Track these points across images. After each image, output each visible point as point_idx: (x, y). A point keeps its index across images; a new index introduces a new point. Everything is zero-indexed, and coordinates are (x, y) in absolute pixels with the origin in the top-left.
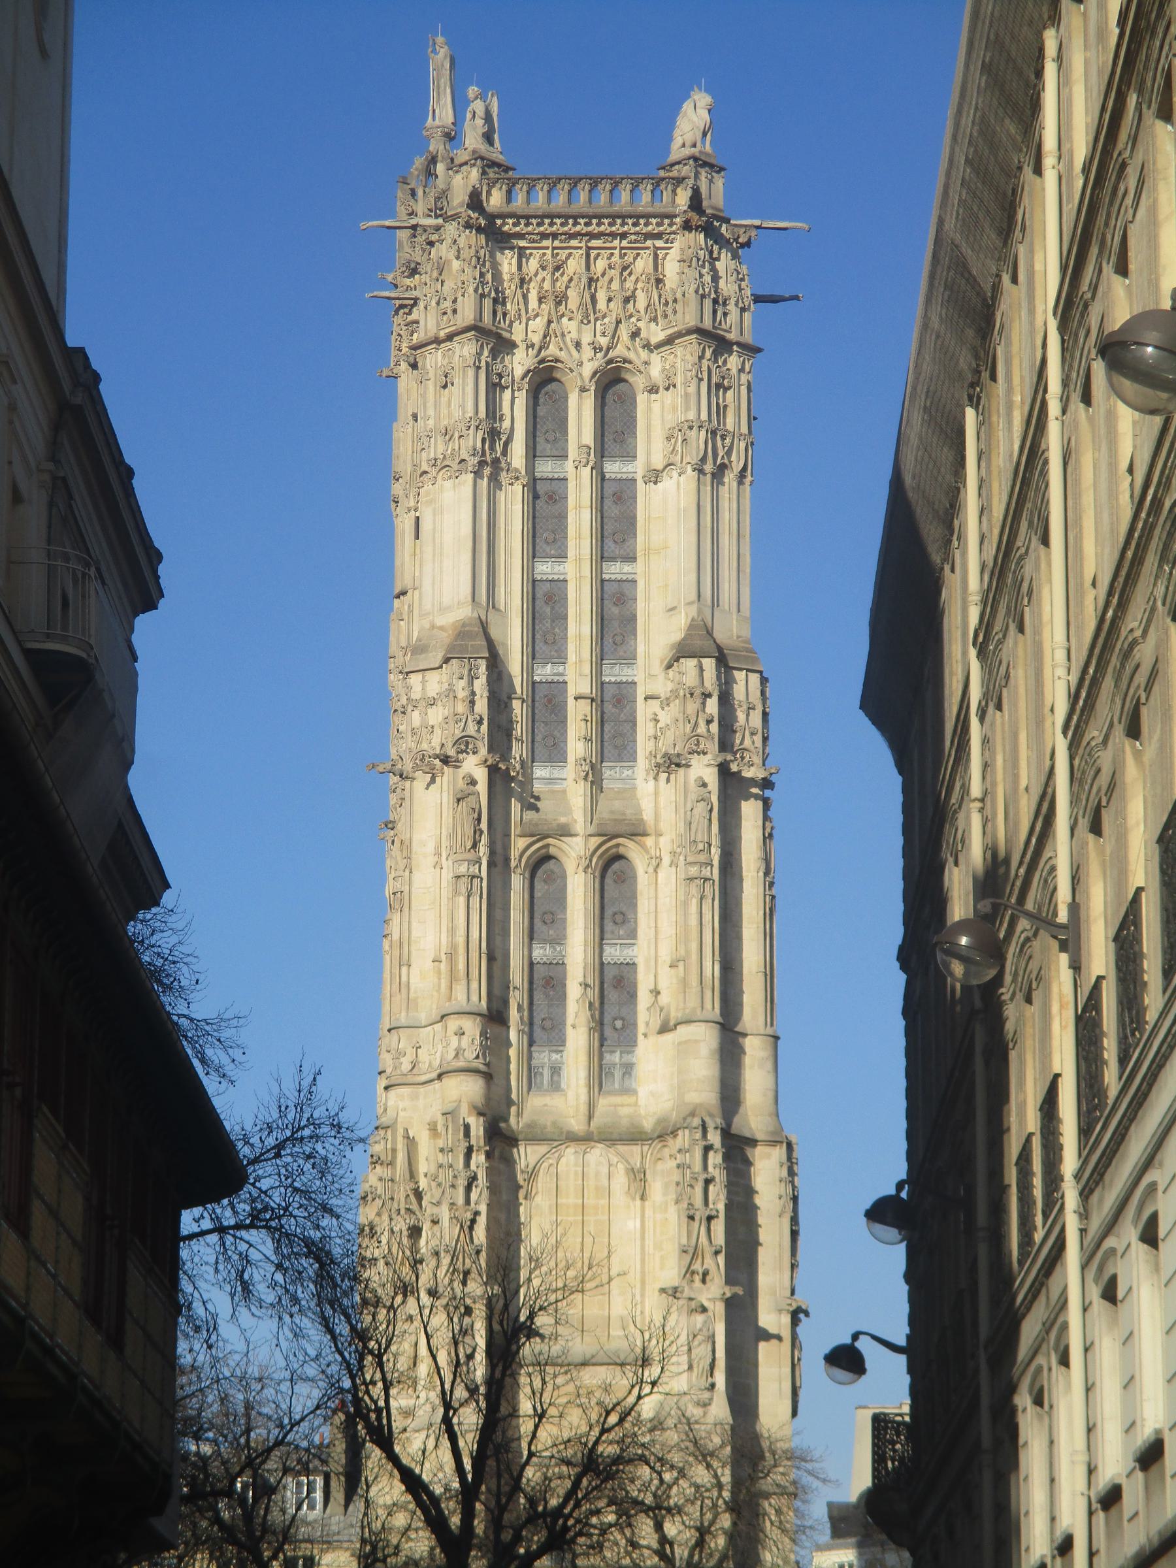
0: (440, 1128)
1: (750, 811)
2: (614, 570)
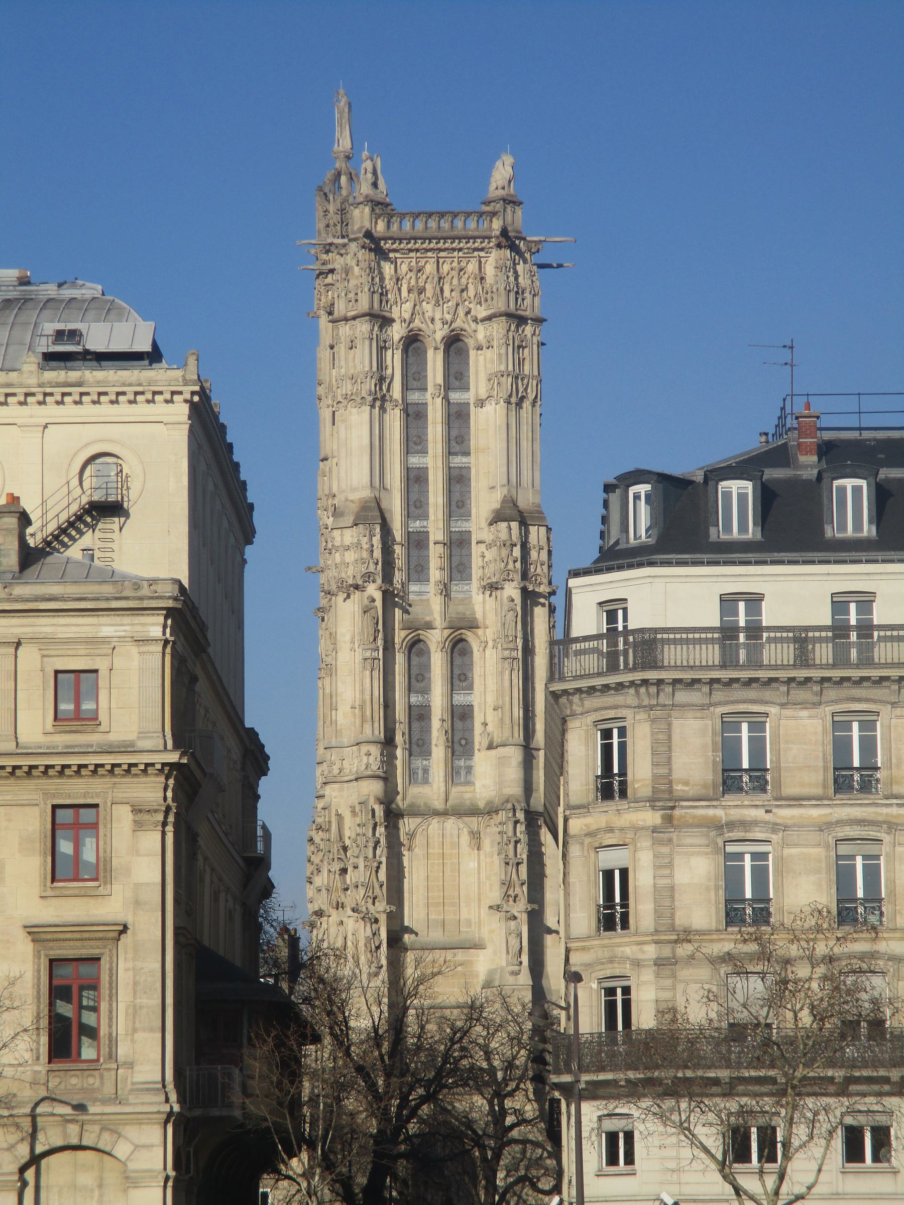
0: (357, 810)
1: (540, 614)
2: (457, 461)
